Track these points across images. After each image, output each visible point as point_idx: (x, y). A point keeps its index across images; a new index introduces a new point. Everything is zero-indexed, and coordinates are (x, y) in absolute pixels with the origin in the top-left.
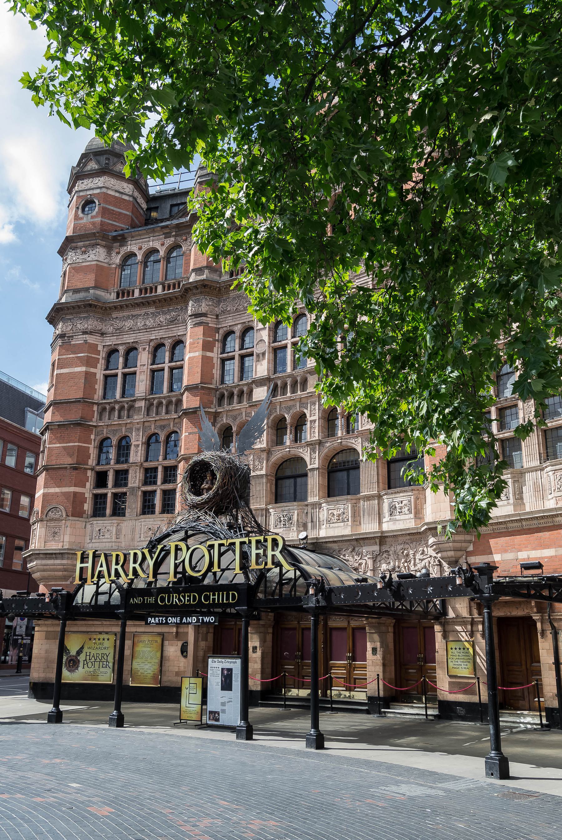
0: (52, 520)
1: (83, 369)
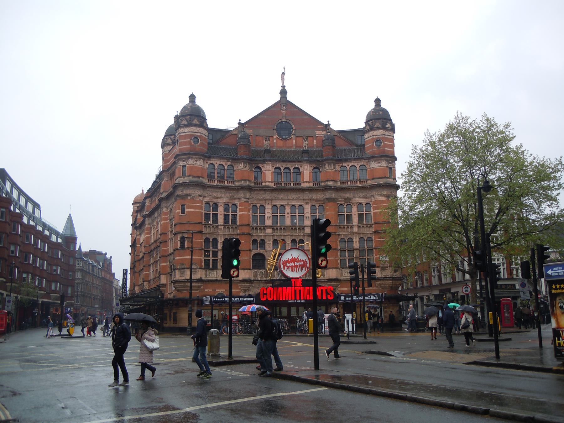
1: (200, 211)
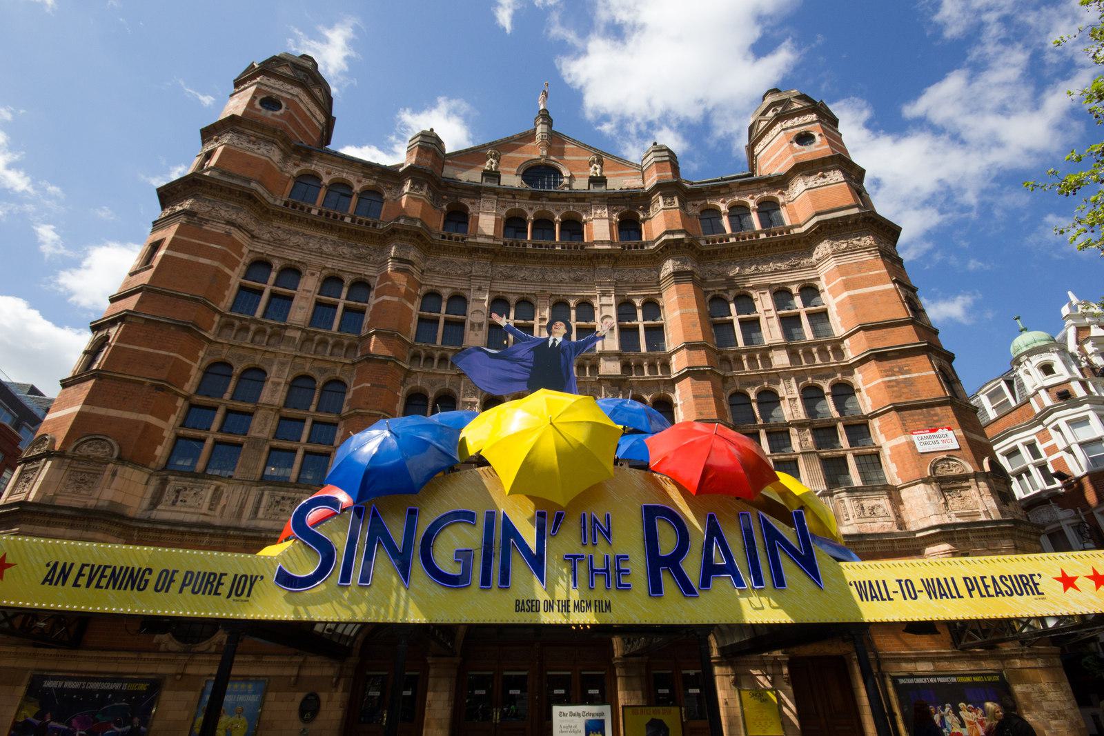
0: (88, 459)
1: (216, 264)
